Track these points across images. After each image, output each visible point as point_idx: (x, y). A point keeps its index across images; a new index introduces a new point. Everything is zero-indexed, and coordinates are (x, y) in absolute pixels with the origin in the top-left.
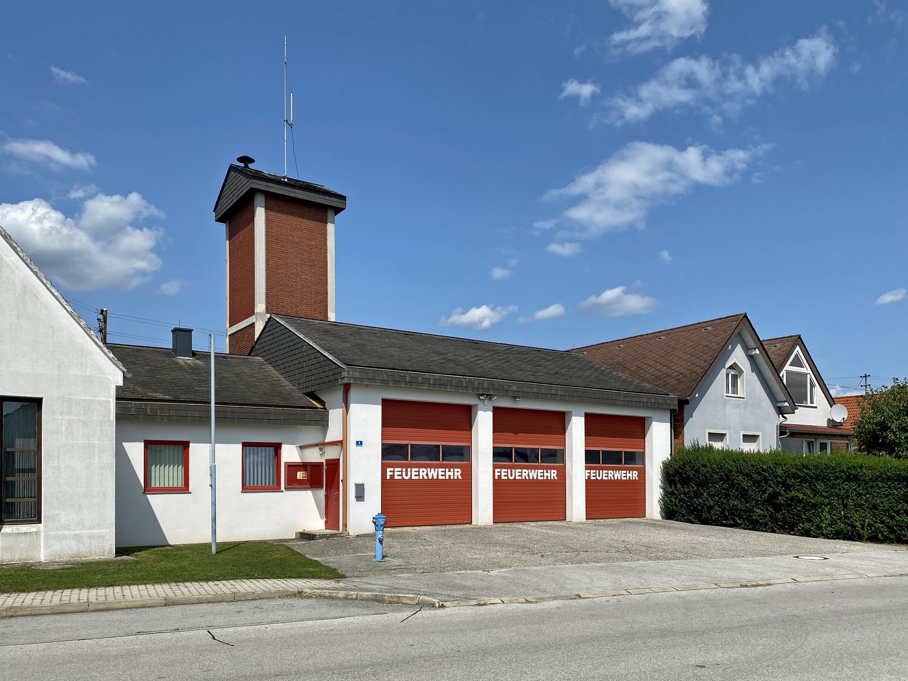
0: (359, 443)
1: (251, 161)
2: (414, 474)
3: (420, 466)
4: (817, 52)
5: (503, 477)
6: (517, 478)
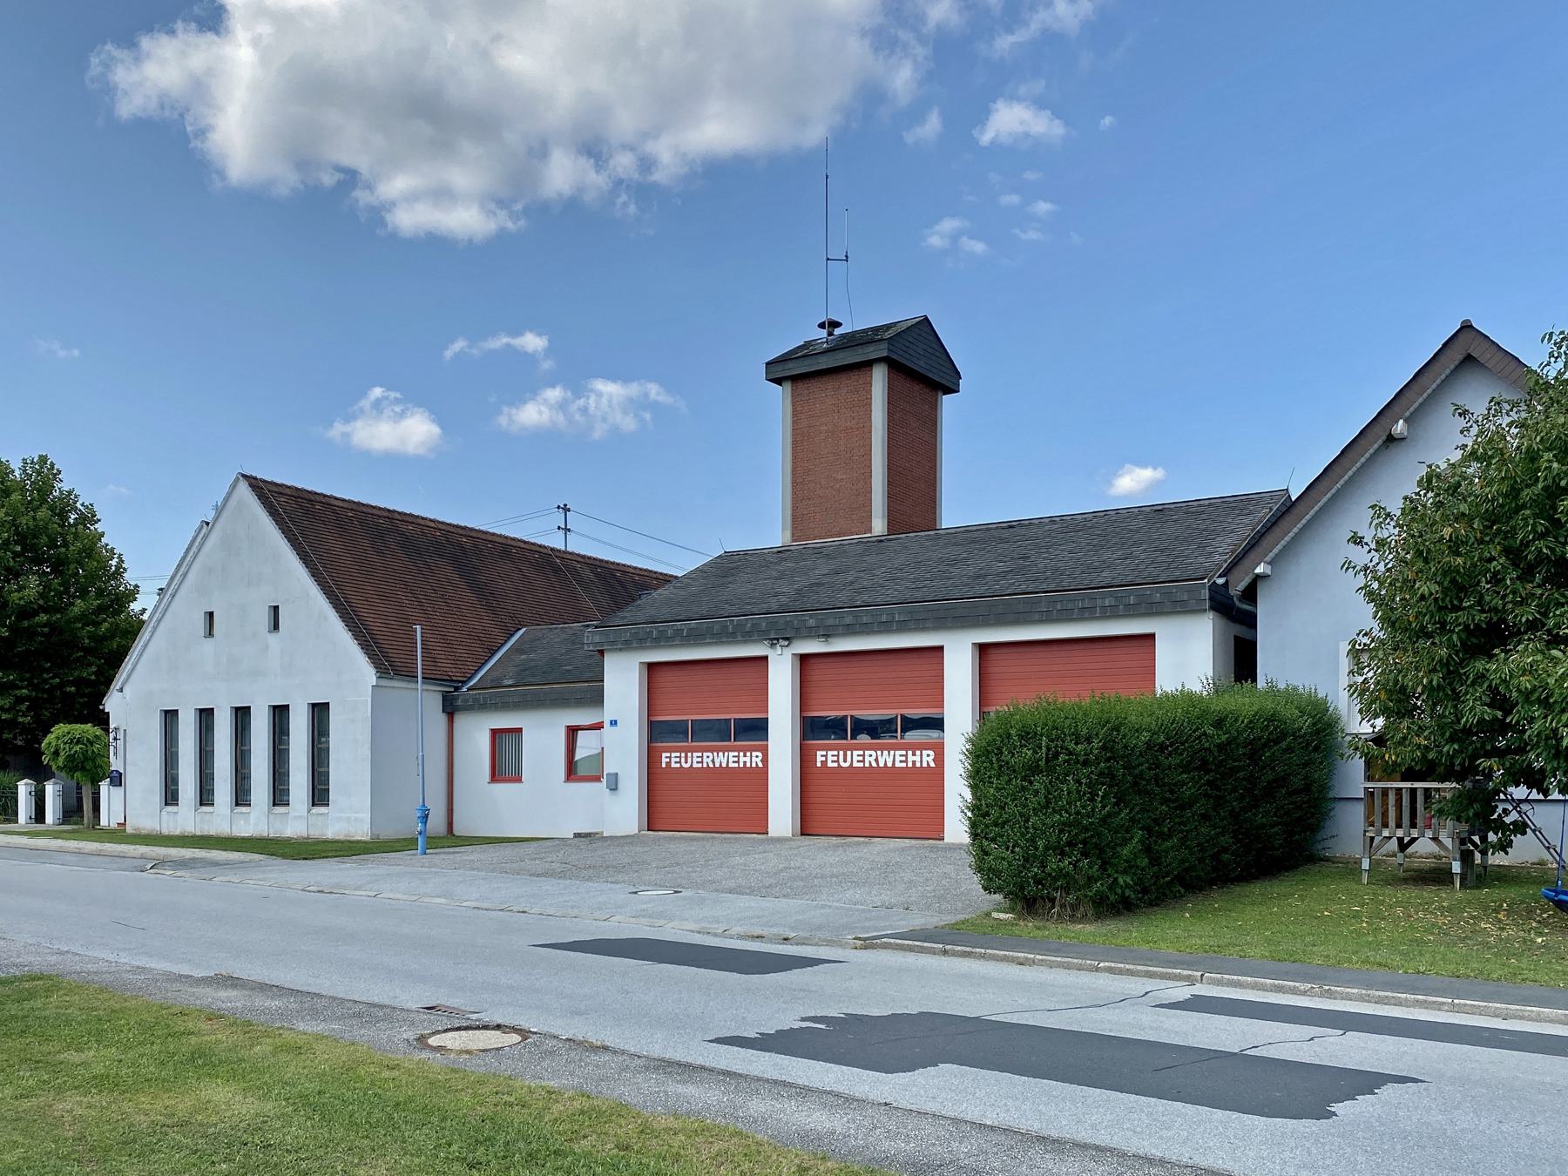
0: (614, 723)
1: (838, 325)
2: (854, 759)
3: (703, 750)
4: (76, 352)
5: (830, 764)
6: (856, 764)
